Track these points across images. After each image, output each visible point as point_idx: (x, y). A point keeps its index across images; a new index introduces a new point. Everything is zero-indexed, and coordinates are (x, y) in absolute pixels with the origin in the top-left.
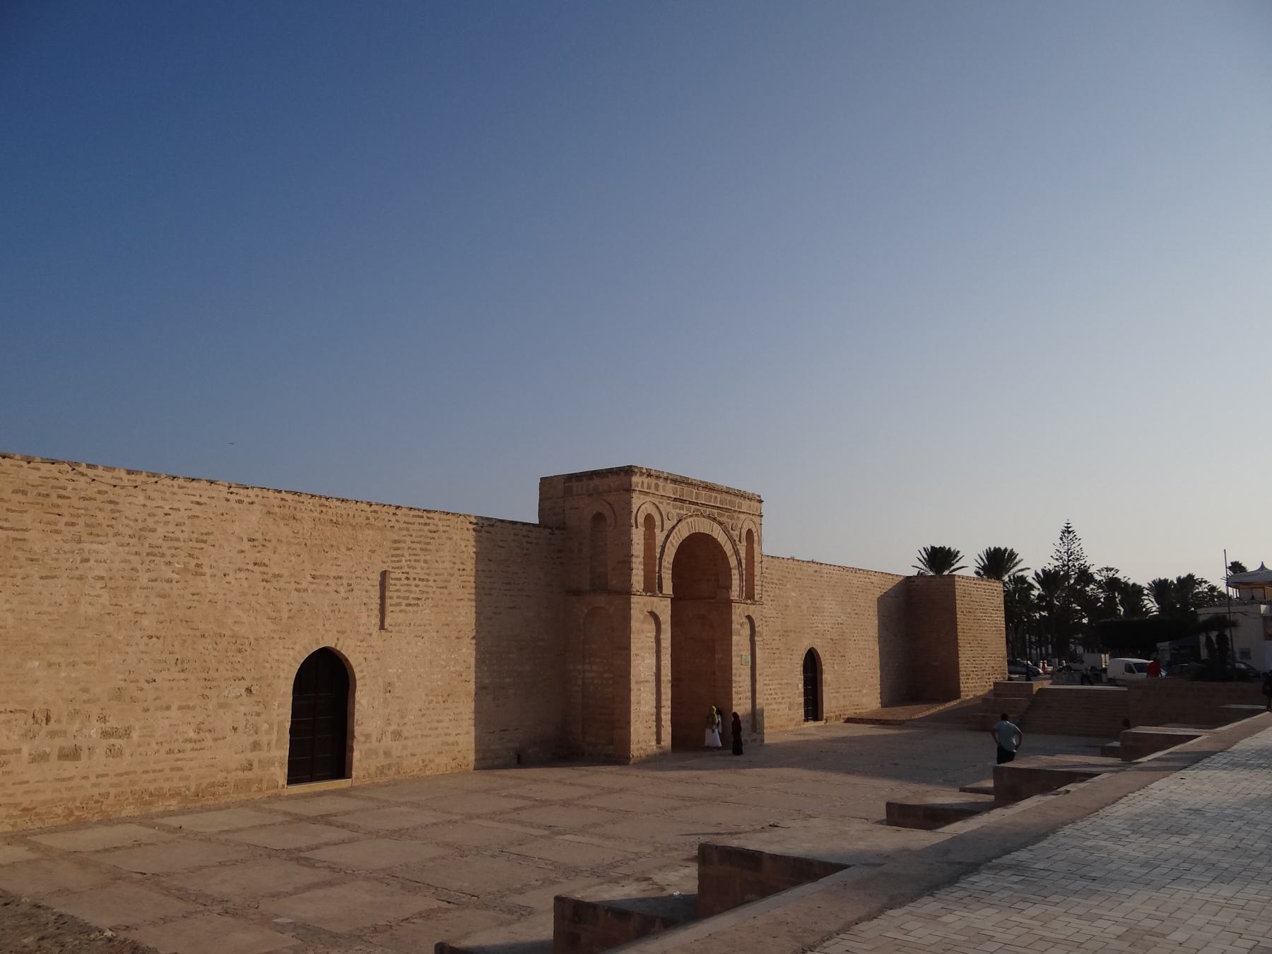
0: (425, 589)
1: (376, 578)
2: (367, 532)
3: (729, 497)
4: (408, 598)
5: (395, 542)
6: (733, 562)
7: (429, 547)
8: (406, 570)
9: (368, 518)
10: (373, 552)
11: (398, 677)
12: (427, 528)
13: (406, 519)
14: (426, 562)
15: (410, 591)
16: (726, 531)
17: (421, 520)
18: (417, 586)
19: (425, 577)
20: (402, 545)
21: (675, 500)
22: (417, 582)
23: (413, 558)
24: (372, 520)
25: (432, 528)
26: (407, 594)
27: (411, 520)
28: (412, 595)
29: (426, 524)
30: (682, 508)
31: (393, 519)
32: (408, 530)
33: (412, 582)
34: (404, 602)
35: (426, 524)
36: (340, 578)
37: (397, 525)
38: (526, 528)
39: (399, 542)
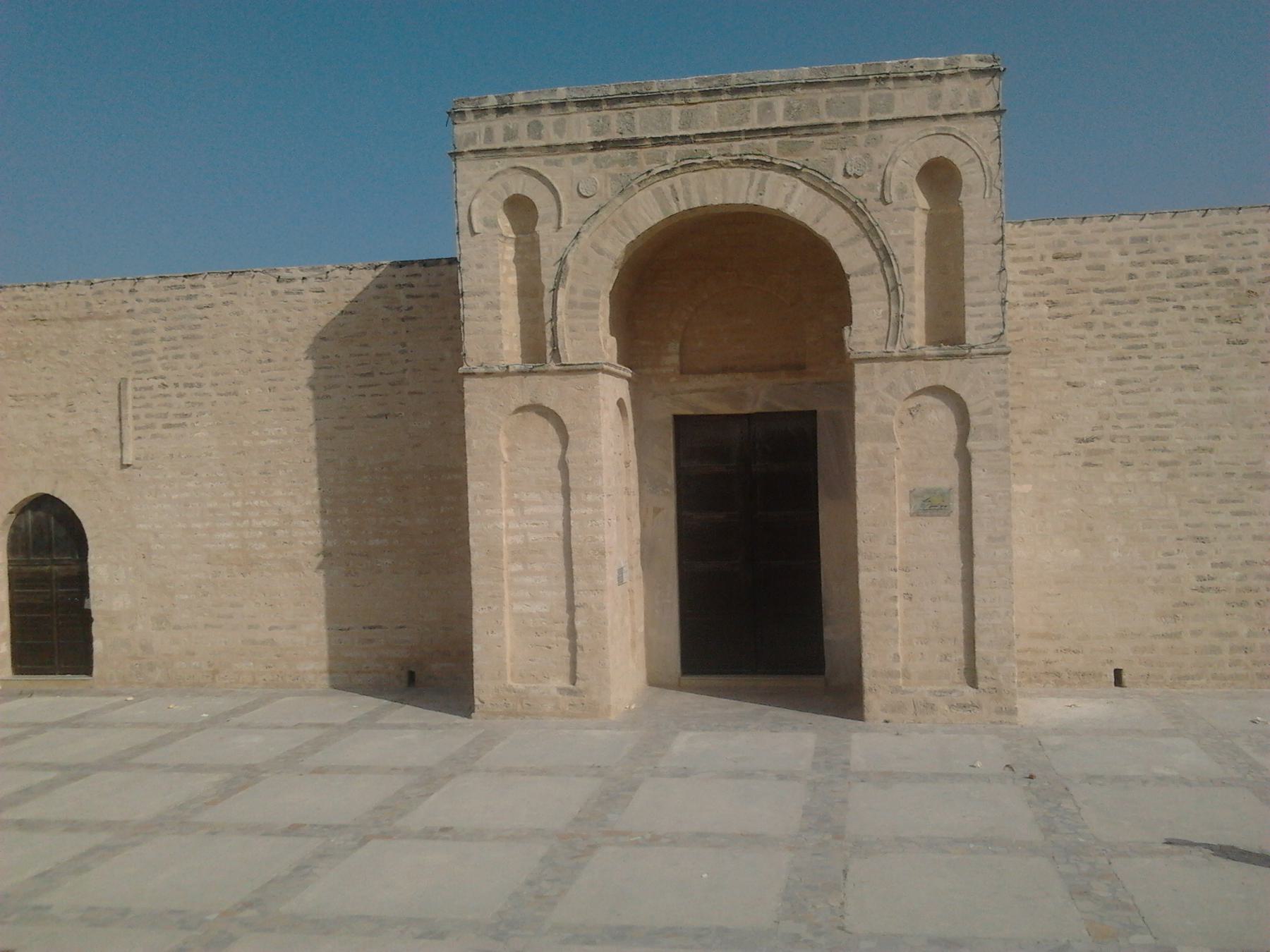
0: (198, 399)
1: (111, 388)
2: (96, 324)
3: (823, 95)
4: (166, 416)
5: (135, 332)
6: (854, 256)
7: (198, 332)
8: (161, 372)
9: (88, 305)
10: (102, 352)
11: (156, 535)
12: (193, 303)
13: (152, 295)
14: (195, 356)
15: (170, 405)
16: (821, 183)
17: (183, 293)
18: (180, 395)
19: (195, 379)
20: (149, 335)
21: (598, 146)
22: (182, 390)
23: (171, 353)
24: (96, 308)
25: (204, 301)
26: (164, 410)
27: (163, 295)
28: (172, 411)
29: (190, 297)
30: (634, 159)
31: (128, 297)
32: (157, 311)
33: (171, 390)
34: (160, 422)
35: (190, 297)
36: (55, 395)
37: (138, 307)
38: (405, 270)
39: (144, 331)
